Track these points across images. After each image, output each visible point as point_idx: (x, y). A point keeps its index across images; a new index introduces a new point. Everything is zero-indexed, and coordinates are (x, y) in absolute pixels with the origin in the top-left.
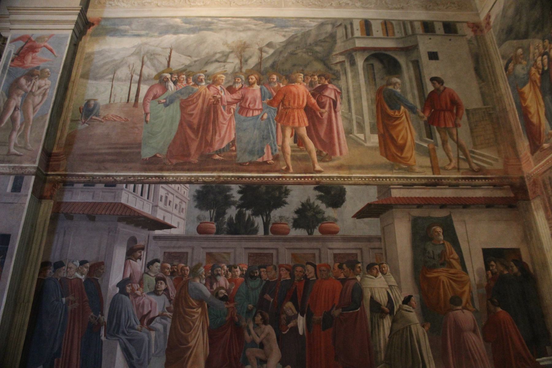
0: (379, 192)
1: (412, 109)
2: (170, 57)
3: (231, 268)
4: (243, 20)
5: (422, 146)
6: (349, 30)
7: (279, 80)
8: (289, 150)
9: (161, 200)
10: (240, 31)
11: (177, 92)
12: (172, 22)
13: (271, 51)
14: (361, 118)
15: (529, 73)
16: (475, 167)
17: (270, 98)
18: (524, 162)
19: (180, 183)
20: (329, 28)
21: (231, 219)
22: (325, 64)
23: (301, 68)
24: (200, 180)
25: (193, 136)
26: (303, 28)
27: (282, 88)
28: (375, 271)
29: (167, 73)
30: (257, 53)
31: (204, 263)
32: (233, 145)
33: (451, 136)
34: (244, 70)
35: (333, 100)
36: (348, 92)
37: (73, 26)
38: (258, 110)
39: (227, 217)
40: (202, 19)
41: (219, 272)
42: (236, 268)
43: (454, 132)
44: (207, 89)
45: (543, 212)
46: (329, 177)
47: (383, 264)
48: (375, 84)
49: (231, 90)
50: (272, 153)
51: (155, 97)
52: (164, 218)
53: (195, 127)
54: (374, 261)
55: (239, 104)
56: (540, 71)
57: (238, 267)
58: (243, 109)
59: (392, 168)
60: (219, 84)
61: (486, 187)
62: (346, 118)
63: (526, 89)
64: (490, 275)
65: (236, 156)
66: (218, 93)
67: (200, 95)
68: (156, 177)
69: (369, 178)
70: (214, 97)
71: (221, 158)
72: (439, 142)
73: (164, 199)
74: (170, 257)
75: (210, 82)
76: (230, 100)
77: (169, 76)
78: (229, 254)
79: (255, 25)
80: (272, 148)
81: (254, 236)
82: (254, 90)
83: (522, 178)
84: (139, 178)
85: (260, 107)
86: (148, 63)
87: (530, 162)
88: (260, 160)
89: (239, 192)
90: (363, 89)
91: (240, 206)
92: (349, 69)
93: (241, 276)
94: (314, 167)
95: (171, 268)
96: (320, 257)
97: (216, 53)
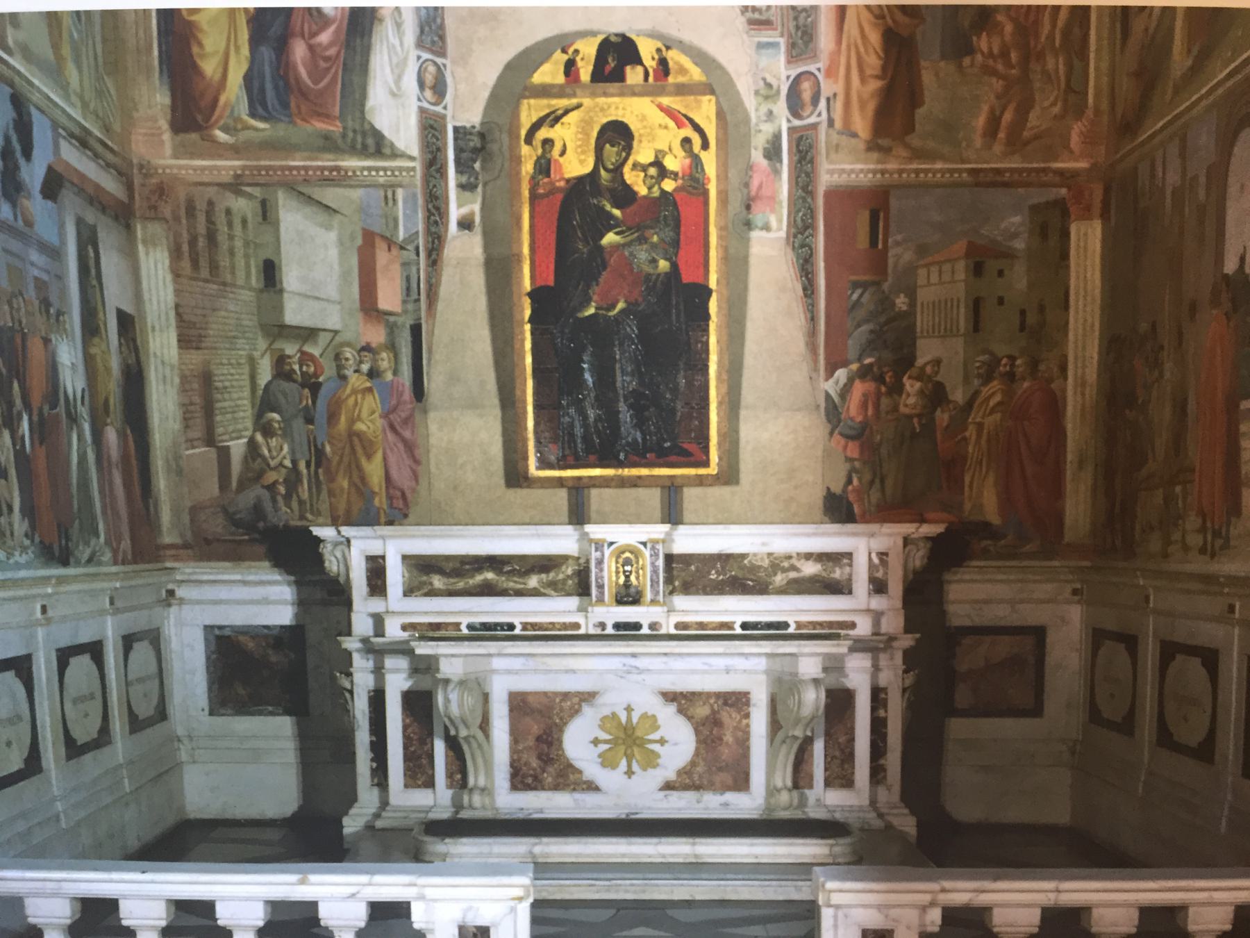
18: (143, 131)
45: (166, 254)
87: (162, 143)
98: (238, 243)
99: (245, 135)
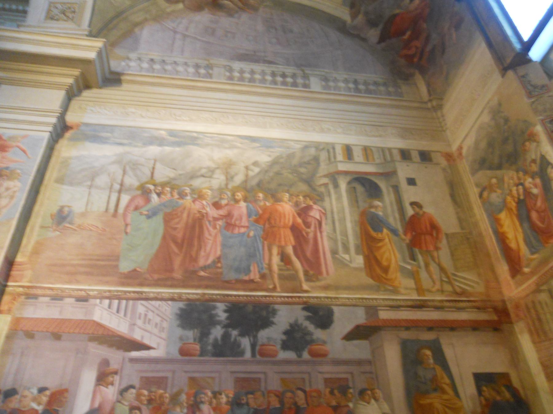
0: (367, 313)
1: (394, 232)
2: (154, 168)
3: (216, 394)
4: (229, 138)
5: (406, 268)
6: (332, 155)
7: (265, 199)
8: (275, 268)
9: (140, 318)
10: (226, 148)
11: (160, 205)
12: (156, 133)
13: (257, 170)
14: (345, 238)
15: (505, 201)
16: (458, 290)
17: (255, 216)
19: (162, 299)
20: (312, 151)
21: (216, 340)
22: (310, 185)
23: (286, 188)
24: (184, 297)
25: (176, 250)
26: (288, 150)
27: (268, 206)
28: (367, 397)
29: (150, 184)
30: (243, 170)
31: (186, 389)
32: (219, 262)
33: (433, 259)
34: (230, 186)
35: (318, 220)
36: (332, 213)
37: (50, 129)
38: (244, 227)
39: (211, 338)
40: (187, 134)
41: (203, 400)
42: (221, 394)
43: (435, 254)
44: (192, 204)
46: (317, 298)
47: (374, 389)
48: (358, 207)
49: (217, 205)
50: (259, 272)
51: (136, 208)
52: (142, 337)
53: (179, 241)
54: (365, 386)
55: (224, 220)
56: (516, 199)
57: (223, 393)
58: (229, 226)
59: (377, 290)
60: (205, 199)
61: (471, 310)
62: (331, 238)
63: (503, 216)
64: (484, 402)
65: (221, 273)
66: (204, 208)
67: (184, 209)
68: (134, 292)
69: (356, 298)
70: (199, 212)
71: (206, 275)
72: (422, 264)
73: (143, 316)
74: (148, 382)
75: (196, 196)
76: (216, 216)
77: (152, 187)
78: (213, 378)
79: (241, 143)
80: (258, 266)
81: (240, 358)
82: (240, 207)
83: (504, 301)
84: (116, 293)
85: (247, 224)
86: (130, 173)
88: (246, 278)
89: (225, 311)
90: (347, 211)
91: (226, 326)
92: (332, 191)
93: (227, 403)
94: (301, 286)
95: (149, 396)
96: (310, 382)
97: (201, 168)
98: (548, 316)
99: (533, 264)
